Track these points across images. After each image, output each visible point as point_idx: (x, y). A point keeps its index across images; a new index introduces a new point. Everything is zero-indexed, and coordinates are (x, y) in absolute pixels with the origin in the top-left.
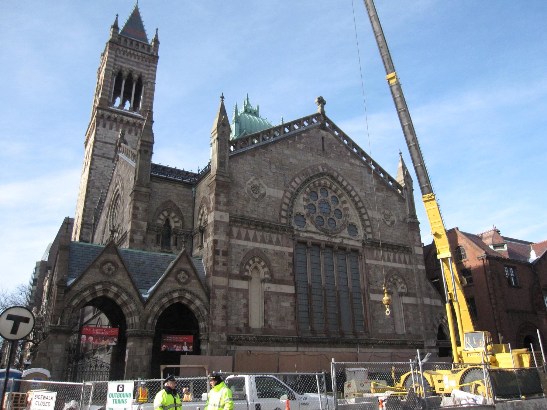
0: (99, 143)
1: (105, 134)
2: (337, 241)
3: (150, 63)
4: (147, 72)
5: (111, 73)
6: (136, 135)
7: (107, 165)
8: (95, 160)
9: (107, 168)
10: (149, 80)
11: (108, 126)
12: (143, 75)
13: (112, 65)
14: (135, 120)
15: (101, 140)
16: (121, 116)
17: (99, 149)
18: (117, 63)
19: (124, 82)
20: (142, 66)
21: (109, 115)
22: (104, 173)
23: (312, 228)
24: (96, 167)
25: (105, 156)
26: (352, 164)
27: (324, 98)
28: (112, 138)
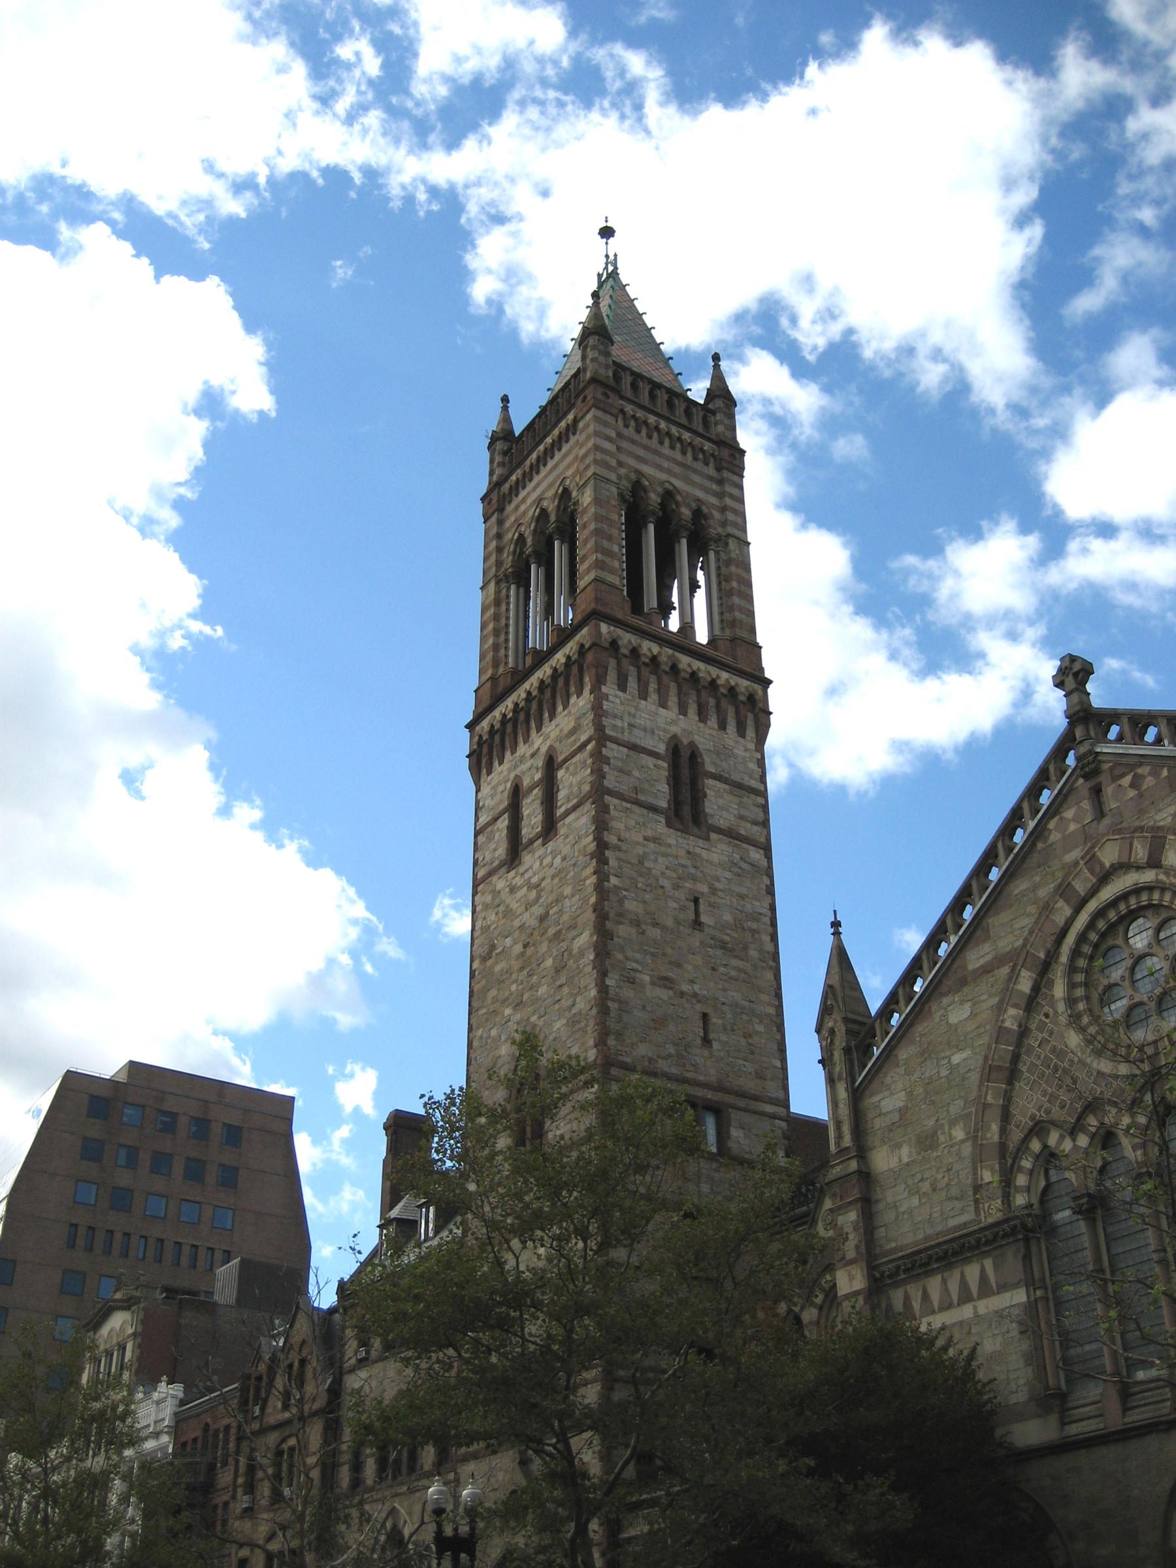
0: (614, 746)
1: (629, 714)
3: (719, 469)
4: (713, 500)
6: (723, 726)
7: (649, 833)
8: (613, 812)
9: (652, 845)
10: (730, 530)
11: (632, 684)
12: (705, 509)
13: (613, 463)
14: (714, 671)
15: (619, 736)
16: (670, 651)
17: (621, 771)
18: (624, 458)
19: (651, 528)
20: (697, 479)
21: (635, 644)
22: (647, 864)
24: (620, 840)
25: (641, 797)
27: (967, 679)
28: (653, 732)
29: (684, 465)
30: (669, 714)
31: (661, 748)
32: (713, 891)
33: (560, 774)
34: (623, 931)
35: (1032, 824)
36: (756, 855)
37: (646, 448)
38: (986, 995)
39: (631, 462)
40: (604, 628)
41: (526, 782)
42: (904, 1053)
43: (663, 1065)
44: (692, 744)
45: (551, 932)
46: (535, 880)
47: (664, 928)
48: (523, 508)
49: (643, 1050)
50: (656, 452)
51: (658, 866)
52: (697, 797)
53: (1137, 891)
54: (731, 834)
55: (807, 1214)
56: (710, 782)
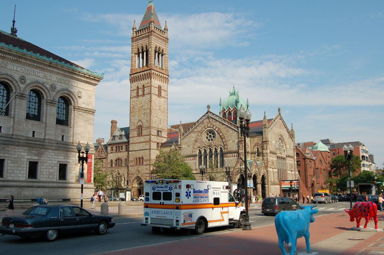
2: (282, 155)
4: (165, 48)
5: (154, 49)
10: (166, 53)
23: (279, 152)
26: (285, 130)
29: (162, 43)
30: (158, 82)
31: (157, 87)
32: (162, 105)
33: (145, 88)
34: (153, 111)
35: (202, 120)
36: (166, 100)
37: (157, 40)
38: (196, 134)
39: (156, 43)
40: (152, 71)
41: (139, 87)
42: (187, 137)
43: (156, 127)
44: (161, 86)
45: (143, 109)
46: (141, 101)
47: (157, 110)
48: (138, 43)
49: (154, 125)
50: (158, 41)
51: (156, 102)
52: (161, 93)
53: (211, 129)
54: (164, 97)
55: (171, 145)
56: (162, 91)
